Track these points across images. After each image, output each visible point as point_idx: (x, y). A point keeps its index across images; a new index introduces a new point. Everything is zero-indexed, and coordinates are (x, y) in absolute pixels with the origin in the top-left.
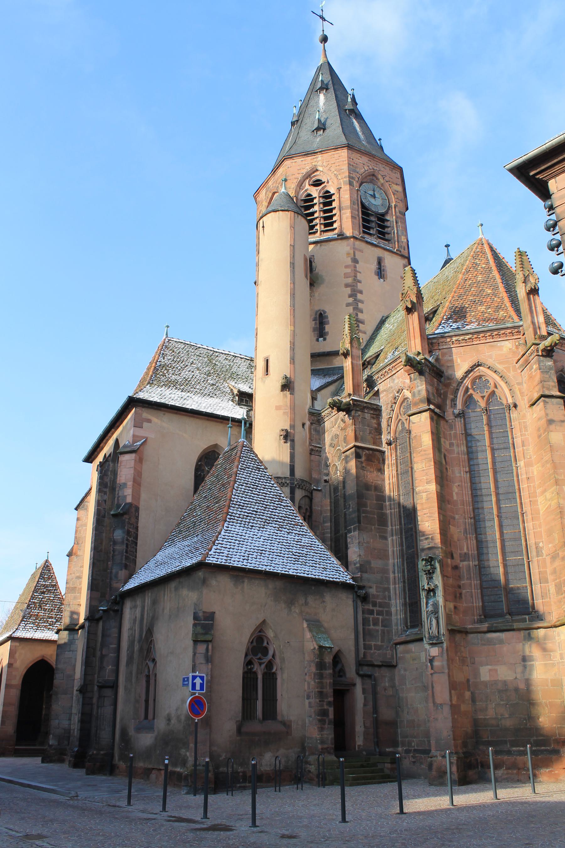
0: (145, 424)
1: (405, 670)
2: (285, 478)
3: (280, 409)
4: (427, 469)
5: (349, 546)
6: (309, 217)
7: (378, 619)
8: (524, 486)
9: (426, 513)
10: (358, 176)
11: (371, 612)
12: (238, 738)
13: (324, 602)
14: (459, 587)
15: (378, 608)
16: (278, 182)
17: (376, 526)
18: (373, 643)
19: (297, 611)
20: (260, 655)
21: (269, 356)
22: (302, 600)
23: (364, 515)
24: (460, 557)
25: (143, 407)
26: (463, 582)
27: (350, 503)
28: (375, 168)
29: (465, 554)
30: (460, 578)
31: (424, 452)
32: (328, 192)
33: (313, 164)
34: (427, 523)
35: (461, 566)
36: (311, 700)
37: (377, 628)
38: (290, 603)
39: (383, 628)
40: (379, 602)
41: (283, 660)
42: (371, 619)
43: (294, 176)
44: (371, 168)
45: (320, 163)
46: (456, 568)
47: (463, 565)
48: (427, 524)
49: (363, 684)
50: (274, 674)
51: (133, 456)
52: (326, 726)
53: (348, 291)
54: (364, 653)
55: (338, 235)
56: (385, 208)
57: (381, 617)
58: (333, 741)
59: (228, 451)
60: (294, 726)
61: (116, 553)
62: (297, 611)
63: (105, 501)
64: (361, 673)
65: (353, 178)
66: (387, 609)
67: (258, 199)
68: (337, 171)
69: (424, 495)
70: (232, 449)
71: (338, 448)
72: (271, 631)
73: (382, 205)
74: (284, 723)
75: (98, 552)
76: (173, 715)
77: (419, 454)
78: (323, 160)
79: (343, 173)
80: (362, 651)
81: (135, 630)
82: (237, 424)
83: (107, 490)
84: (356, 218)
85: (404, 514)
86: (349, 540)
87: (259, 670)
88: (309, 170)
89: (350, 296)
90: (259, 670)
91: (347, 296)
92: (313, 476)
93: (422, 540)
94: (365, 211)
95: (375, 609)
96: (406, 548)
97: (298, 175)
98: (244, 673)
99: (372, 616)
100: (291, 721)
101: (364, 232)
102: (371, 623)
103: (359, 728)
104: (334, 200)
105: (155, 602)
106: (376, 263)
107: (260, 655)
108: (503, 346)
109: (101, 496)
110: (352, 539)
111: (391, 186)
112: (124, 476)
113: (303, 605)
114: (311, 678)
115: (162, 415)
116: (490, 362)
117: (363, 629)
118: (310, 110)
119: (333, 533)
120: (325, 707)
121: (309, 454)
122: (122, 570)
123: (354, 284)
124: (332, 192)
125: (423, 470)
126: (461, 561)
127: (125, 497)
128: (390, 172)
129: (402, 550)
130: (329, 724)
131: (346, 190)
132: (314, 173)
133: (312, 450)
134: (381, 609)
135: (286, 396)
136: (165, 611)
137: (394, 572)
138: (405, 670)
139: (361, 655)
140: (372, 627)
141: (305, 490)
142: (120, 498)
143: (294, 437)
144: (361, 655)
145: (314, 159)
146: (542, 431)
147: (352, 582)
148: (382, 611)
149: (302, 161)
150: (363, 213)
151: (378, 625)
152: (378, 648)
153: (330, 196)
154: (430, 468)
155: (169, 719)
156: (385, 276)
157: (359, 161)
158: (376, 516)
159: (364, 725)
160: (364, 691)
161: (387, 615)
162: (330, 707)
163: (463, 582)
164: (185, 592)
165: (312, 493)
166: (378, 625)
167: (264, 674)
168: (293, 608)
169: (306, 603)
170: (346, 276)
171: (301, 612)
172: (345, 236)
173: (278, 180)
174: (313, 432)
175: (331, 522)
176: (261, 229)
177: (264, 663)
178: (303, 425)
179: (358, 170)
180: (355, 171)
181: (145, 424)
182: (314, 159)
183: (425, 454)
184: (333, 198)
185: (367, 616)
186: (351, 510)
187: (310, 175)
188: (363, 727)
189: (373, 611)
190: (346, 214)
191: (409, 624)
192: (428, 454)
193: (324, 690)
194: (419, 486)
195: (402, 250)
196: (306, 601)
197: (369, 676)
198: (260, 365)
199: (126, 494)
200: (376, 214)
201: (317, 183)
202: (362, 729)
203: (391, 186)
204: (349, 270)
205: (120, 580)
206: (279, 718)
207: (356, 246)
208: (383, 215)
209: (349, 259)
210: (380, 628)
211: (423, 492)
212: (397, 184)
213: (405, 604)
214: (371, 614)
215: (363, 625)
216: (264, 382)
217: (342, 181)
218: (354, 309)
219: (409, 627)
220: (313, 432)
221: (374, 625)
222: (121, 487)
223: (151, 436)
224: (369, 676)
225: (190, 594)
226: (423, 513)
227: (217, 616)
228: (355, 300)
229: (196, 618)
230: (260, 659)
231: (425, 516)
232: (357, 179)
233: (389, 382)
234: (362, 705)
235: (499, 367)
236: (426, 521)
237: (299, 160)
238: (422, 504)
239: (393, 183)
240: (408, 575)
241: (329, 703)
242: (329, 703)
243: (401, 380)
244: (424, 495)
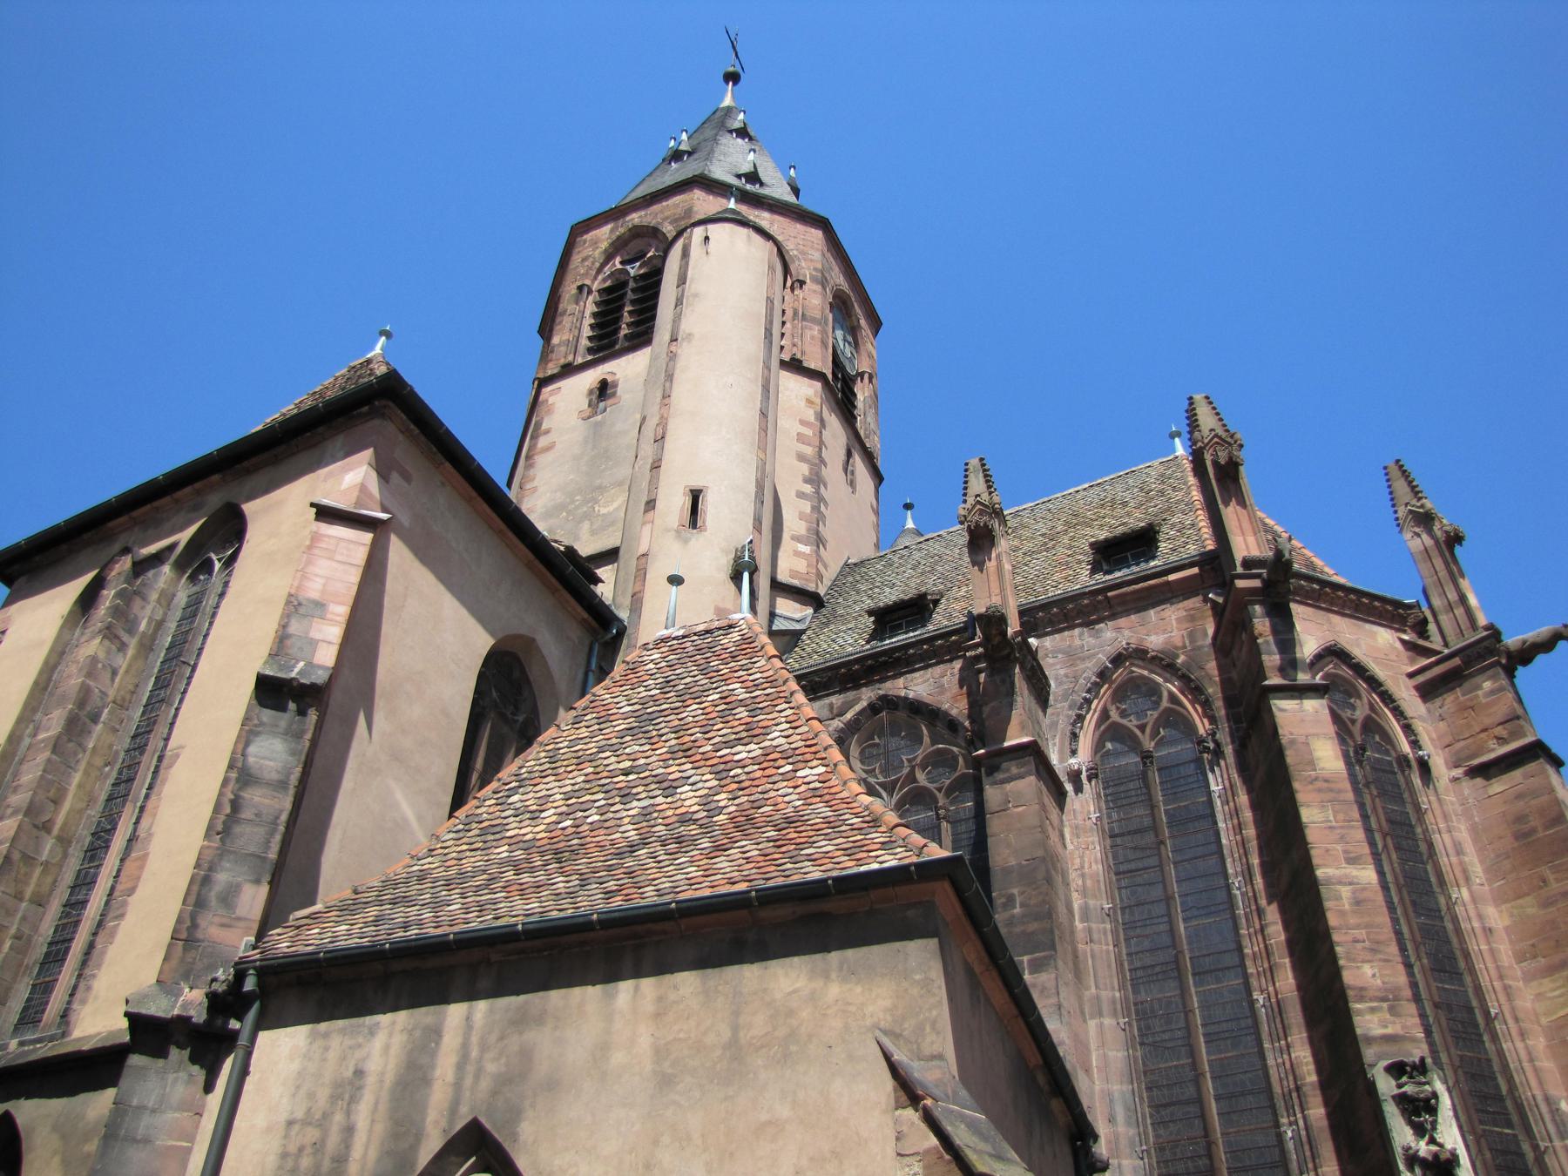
4: (1342, 827)
8: (1477, 946)
9: (1361, 938)
27: (1015, 891)
31: (1326, 785)
48: (1367, 970)
51: (367, 537)
53: (805, 469)
61: (247, 814)
63: (114, 673)
69: (1345, 892)
75: (35, 826)
77: (1310, 787)
81: (349, 1130)
82: (586, 615)
83: (133, 643)
89: (807, 481)
91: (801, 478)
93: (1360, 1012)
108: (1376, 633)
109: (108, 652)
115: (439, 483)
116: (1359, 653)
122: (257, 882)
125: (1330, 827)
127: (314, 644)
136: (618, 1058)
137: (1111, 1120)
142: (288, 642)
146: (1535, 822)
154: (1352, 827)
170: (801, 438)
181: (395, 477)
183: (1331, 790)
186: (1017, 910)
190: (811, 329)
192: (1340, 791)
194: (1325, 866)
198: (673, 504)
199: (315, 634)
204: (808, 432)
205: (239, 919)
209: (811, 412)
211: (1340, 883)
216: (686, 541)
218: (813, 508)
222: (302, 610)
225: (834, 990)
228: (817, 492)
231: (1359, 946)
233: (1081, 635)
235: (1380, 672)
236: (1363, 962)
238: (1342, 913)
243: (1127, 633)
244: (1345, 892)
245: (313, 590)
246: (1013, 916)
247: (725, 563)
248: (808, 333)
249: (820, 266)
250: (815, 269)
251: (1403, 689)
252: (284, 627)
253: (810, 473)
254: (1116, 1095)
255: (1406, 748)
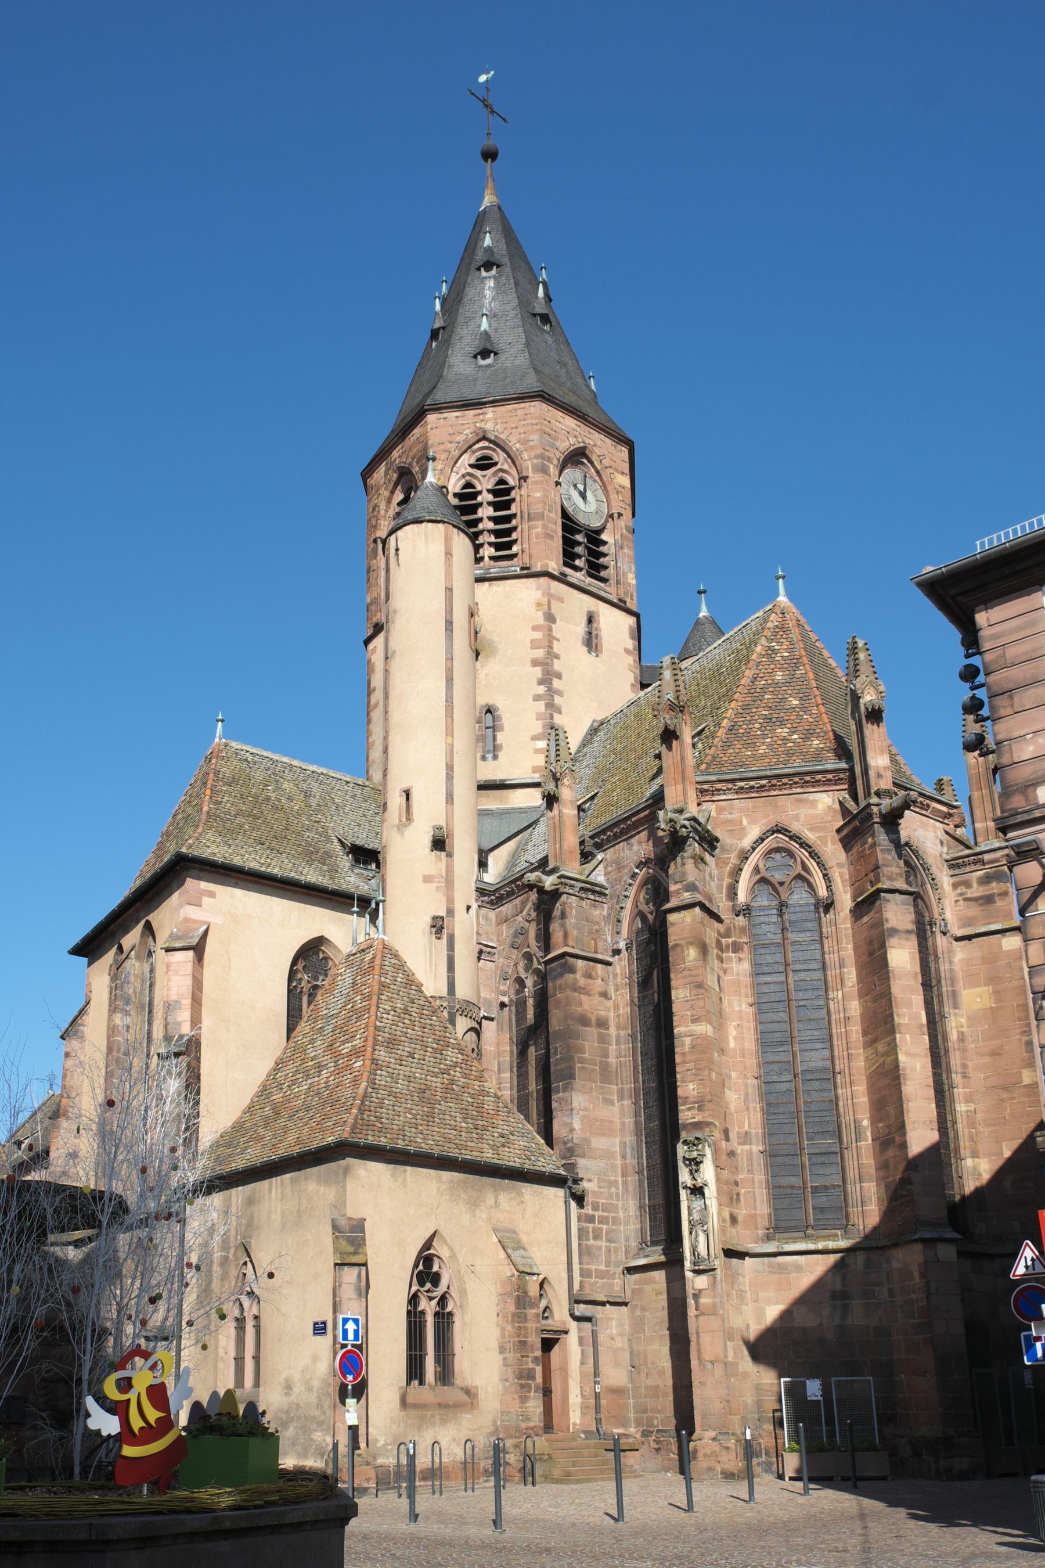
0: (206, 900)
1: (643, 1309)
2: (441, 998)
3: (432, 882)
5: (554, 1114)
6: (471, 529)
7: (601, 1229)
10: (558, 454)
11: (591, 1219)
12: (403, 1413)
13: (522, 1202)
14: (736, 1183)
15: (600, 1213)
16: (411, 454)
17: (599, 1083)
18: (594, 1267)
19: (484, 1217)
20: (428, 1285)
21: (412, 787)
22: (490, 1200)
23: (580, 1065)
24: (738, 1138)
25: (201, 870)
26: (741, 1177)
27: (558, 1045)
28: (587, 441)
29: (746, 1133)
30: (735, 1169)
32: (502, 482)
33: (478, 425)
34: (691, 1084)
35: (739, 1151)
36: (507, 1355)
37: (599, 1243)
38: (474, 1204)
39: (608, 1244)
40: (603, 1204)
41: (463, 1292)
42: (590, 1230)
43: (442, 447)
44: (580, 440)
45: (489, 426)
46: (732, 1154)
47: (742, 1150)
49: (579, 1330)
50: (450, 1314)
52: (532, 1394)
54: (581, 1282)
55: (522, 569)
56: (601, 517)
57: (605, 1227)
58: (542, 1417)
59: (355, 954)
60: (481, 1395)
62: (484, 1217)
64: (577, 1313)
65: (549, 460)
66: (614, 1215)
67: (371, 482)
68: (522, 444)
70: (363, 950)
71: (525, 950)
72: (445, 1247)
73: (597, 513)
74: (467, 1391)
76: (296, 1380)
78: (497, 418)
79: (532, 447)
80: (577, 1279)
84: (553, 537)
85: (642, 1066)
86: (554, 1105)
87: (428, 1307)
88: (470, 436)
90: (428, 1307)
92: (483, 995)
94: (569, 525)
95: (596, 1214)
96: (645, 1119)
97: (449, 445)
98: (409, 1313)
99: (592, 1225)
100: (477, 1387)
101: (566, 564)
102: (591, 1237)
103: (575, 1398)
104: (513, 500)
105: (251, 1201)
106: (584, 620)
107: (428, 1285)
110: (560, 1104)
111: (612, 476)
112: (176, 989)
113: (492, 1207)
114: (507, 1321)
117: (580, 1245)
118: (465, 310)
119: (515, 1089)
120: (531, 1365)
121: (476, 959)
123: (549, 661)
124: (512, 482)
126: (739, 1144)
127: (179, 1024)
128: (612, 449)
129: (637, 1123)
130: (535, 1392)
131: (536, 483)
132: (478, 442)
133: (481, 952)
134: (605, 1214)
135: (441, 860)
137: (624, 1157)
138: (643, 1309)
139: (576, 1287)
140: (591, 1242)
141: (471, 1018)
142: (169, 1027)
143: (453, 930)
144: (576, 1287)
145: (479, 415)
147: (563, 1173)
148: (607, 1218)
149: (457, 417)
150: (565, 528)
151: (601, 1239)
152: (600, 1274)
153: (508, 491)
155: (288, 1387)
156: (599, 647)
157: (560, 426)
158: (598, 1068)
159: (582, 1394)
160: (581, 1341)
161: (614, 1224)
162: (538, 1365)
163: (741, 1177)
164: (312, 1186)
165: (480, 1024)
166: (601, 1239)
167: (437, 1314)
168: (478, 1211)
169: (497, 1205)
171: (490, 1218)
172: (533, 570)
173: (410, 449)
174: (482, 922)
175: (511, 1071)
176: (392, 552)
177: (434, 1298)
178: (468, 908)
179: (558, 444)
180: (553, 446)
181: (206, 900)
182: (479, 415)
184: (513, 494)
185: (584, 1224)
187: (470, 447)
188: (580, 1396)
189: (593, 1217)
190: (536, 528)
191: (649, 1239)
193: (529, 1339)
195: (628, 600)
196: (496, 1201)
197: (589, 1319)
199: (179, 1019)
200: (586, 529)
201: (484, 464)
202: (579, 1399)
203: (612, 476)
206: (458, 1381)
207: (552, 591)
208: (600, 531)
210: (603, 1243)
212: (623, 473)
213: (641, 1207)
214: (590, 1223)
215: (579, 1239)
217: (529, 463)
219: (649, 1244)
220: (482, 922)
221: (595, 1238)
222: (171, 1008)
223: (215, 920)
224: (589, 1319)
226: (685, 1069)
227: (367, 1225)
229: (335, 1228)
230: (428, 1291)
232: (555, 462)
234: (578, 1364)
237: (452, 415)
239: (617, 471)
240: (648, 1163)
241: (536, 1360)
242: (536, 1360)
245: (173, 997)
246: (557, 1059)
247: (427, 841)
248: (534, 532)
249: (539, 451)
250: (536, 457)
251: (829, 844)
252: (166, 1019)
253: (543, 675)
254: (628, 1143)
255: (822, 892)
